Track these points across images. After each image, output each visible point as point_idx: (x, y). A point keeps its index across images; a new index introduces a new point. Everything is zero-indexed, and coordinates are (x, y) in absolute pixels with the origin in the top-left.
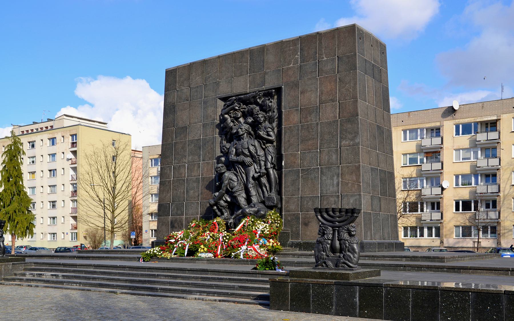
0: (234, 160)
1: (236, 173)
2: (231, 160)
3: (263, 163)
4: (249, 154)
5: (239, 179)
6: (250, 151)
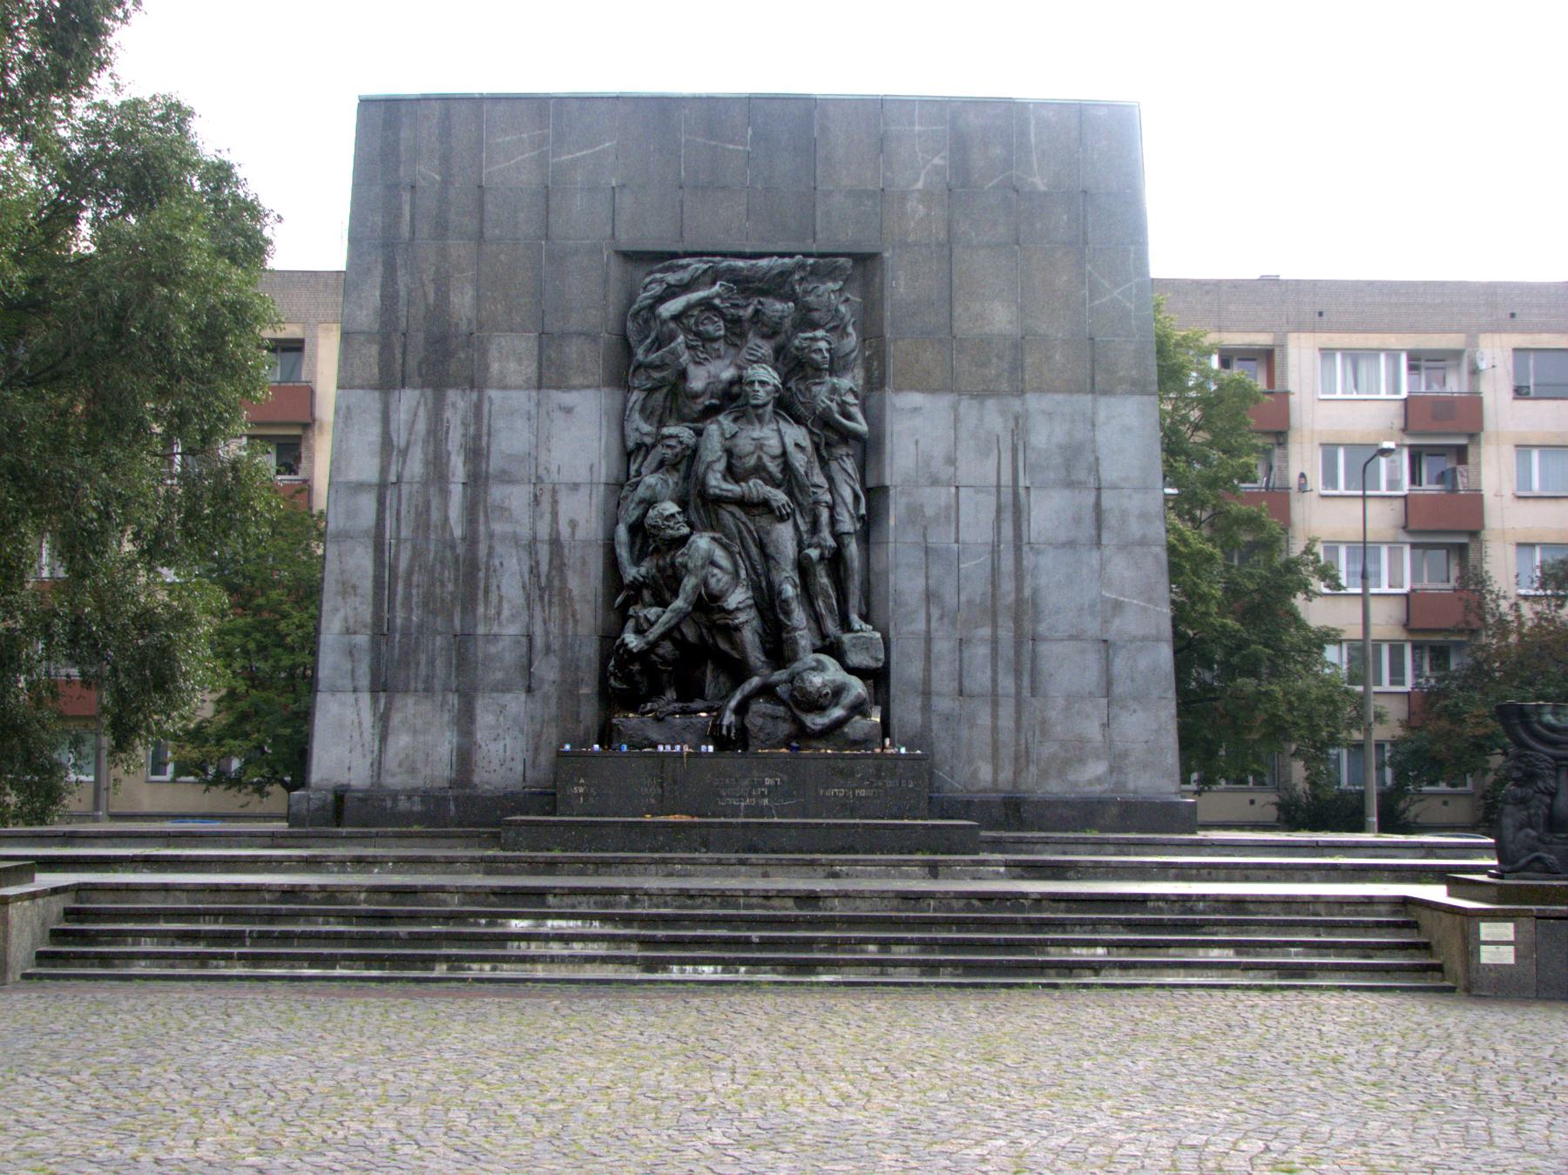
0: (730, 494)
1: (725, 540)
2: (717, 491)
3: (825, 515)
4: (780, 476)
5: (740, 562)
6: (787, 467)
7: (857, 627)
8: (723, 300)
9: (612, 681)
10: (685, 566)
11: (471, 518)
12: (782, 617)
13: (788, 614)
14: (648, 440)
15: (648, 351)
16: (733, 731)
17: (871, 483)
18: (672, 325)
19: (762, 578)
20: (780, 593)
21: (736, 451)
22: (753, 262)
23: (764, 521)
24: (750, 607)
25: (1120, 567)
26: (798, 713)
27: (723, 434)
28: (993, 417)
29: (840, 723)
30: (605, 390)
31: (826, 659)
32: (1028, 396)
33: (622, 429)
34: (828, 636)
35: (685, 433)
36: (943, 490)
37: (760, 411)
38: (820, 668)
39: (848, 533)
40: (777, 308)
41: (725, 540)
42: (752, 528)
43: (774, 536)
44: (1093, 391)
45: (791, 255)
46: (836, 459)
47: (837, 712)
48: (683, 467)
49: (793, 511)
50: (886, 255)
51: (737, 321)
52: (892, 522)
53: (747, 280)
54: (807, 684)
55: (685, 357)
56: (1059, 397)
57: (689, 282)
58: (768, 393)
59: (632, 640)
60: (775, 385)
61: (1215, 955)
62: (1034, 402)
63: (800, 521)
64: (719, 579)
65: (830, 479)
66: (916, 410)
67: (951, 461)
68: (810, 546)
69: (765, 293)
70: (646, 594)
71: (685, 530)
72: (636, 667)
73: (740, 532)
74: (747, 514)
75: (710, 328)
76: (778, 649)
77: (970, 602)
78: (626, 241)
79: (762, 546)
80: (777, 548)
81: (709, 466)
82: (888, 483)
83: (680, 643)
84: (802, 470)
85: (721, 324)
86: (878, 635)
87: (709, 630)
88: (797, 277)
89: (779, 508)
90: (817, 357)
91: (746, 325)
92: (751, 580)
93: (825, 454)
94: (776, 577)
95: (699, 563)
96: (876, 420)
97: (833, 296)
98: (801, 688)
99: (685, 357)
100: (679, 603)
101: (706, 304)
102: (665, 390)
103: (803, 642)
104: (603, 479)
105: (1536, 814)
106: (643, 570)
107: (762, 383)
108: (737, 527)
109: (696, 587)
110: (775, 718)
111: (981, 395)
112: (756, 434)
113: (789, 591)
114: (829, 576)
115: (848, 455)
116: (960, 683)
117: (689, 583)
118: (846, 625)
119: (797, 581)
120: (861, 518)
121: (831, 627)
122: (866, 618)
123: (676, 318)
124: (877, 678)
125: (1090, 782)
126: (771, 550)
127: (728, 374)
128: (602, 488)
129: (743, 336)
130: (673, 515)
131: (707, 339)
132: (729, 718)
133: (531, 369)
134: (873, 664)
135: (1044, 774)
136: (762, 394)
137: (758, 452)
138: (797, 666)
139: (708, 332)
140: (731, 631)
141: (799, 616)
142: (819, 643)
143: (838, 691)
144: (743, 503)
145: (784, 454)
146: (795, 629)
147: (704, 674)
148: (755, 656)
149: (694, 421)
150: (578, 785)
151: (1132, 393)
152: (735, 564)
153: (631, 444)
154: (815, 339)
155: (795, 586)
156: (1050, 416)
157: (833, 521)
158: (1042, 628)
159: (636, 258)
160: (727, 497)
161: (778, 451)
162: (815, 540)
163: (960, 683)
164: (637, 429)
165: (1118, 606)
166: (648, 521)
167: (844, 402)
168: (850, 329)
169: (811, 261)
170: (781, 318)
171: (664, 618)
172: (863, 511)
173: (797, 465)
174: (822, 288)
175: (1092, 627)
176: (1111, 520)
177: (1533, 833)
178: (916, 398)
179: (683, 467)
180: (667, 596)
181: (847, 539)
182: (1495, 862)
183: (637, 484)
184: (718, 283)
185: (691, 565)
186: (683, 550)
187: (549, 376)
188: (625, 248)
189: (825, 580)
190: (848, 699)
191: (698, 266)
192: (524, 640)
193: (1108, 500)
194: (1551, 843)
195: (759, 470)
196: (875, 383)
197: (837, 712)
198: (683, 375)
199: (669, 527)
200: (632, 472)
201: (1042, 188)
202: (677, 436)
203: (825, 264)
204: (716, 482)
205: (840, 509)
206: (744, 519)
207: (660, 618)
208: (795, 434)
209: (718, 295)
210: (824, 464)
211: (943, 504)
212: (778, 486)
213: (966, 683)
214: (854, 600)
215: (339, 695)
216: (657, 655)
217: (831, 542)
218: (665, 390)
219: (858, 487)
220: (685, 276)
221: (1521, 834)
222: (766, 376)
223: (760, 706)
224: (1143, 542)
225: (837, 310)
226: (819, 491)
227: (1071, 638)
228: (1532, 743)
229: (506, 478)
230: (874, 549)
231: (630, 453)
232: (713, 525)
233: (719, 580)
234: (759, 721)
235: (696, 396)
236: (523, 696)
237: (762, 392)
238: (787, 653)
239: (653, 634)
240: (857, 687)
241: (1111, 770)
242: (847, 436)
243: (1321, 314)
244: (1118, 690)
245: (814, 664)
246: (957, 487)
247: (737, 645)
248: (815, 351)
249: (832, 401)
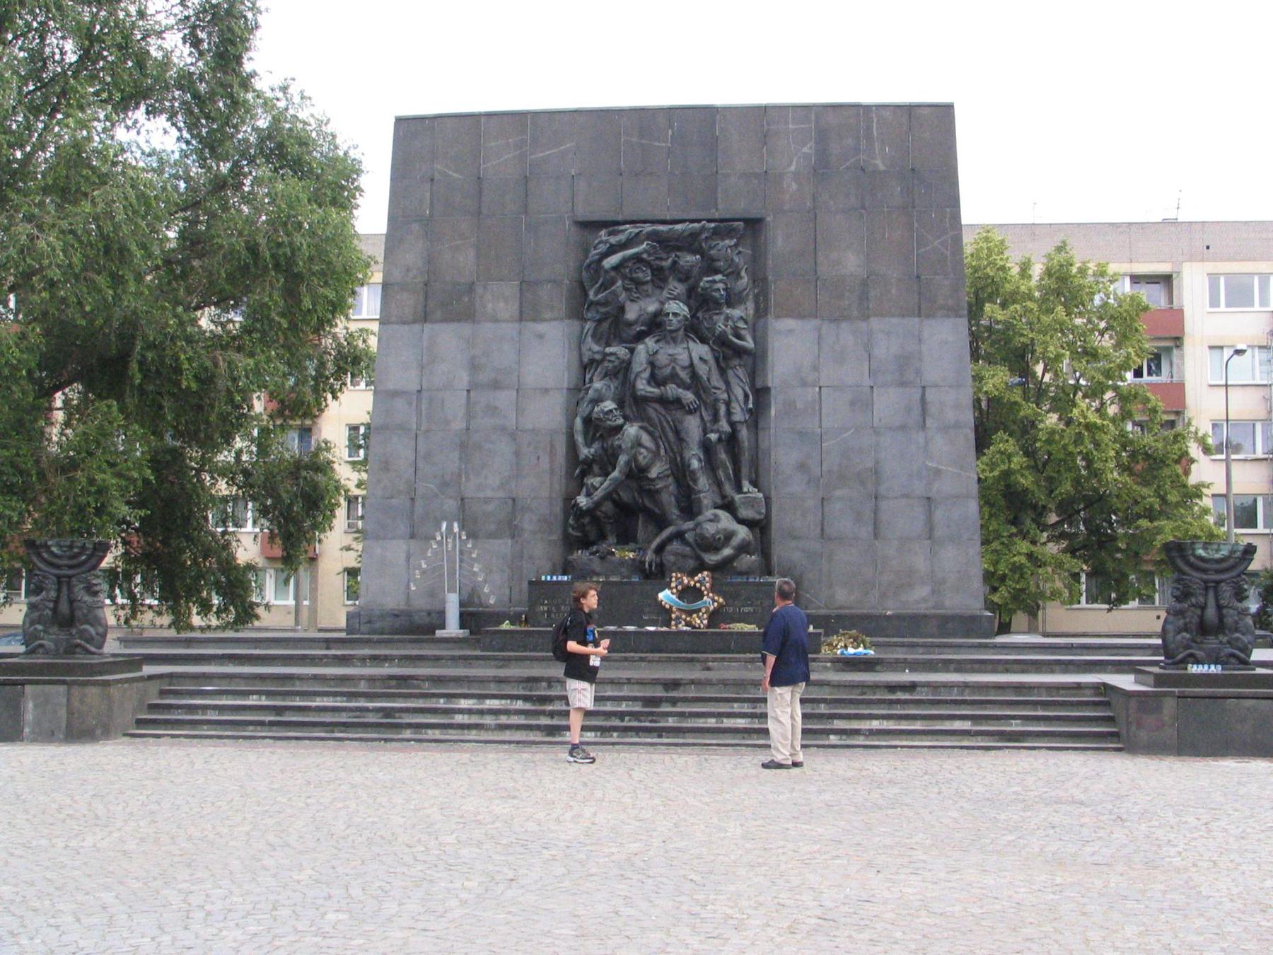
2: (643, 393)
6: (694, 375)
7: (745, 490)
8: (650, 255)
9: (570, 530)
10: (620, 447)
11: (469, 415)
12: (691, 483)
13: (695, 481)
14: (598, 357)
15: (596, 294)
16: (654, 565)
17: (759, 384)
18: (613, 274)
20: (689, 466)
21: (657, 363)
22: (671, 226)
23: (679, 414)
24: (668, 476)
25: (940, 444)
26: (699, 552)
27: (648, 352)
28: (846, 335)
29: (728, 561)
30: (567, 321)
31: (720, 512)
32: (872, 319)
33: (580, 349)
35: (620, 350)
36: (810, 390)
37: (674, 335)
38: (715, 519)
39: (740, 422)
40: (688, 259)
42: (669, 419)
43: (686, 424)
44: (919, 315)
45: (699, 221)
46: (732, 368)
47: (727, 552)
48: (621, 376)
50: (768, 219)
51: (661, 269)
52: (773, 412)
53: (668, 240)
54: (705, 532)
55: (623, 296)
56: (895, 320)
57: (626, 242)
58: (679, 322)
59: (582, 501)
60: (685, 316)
61: (958, 725)
62: (875, 323)
63: (704, 414)
64: (643, 457)
65: (727, 383)
66: (791, 331)
67: (816, 368)
68: (712, 431)
69: (679, 249)
70: (596, 468)
71: (620, 421)
72: (586, 520)
74: (665, 408)
75: (641, 275)
76: (690, 509)
77: (829, 471)
78: (583, 213)
79: (677, 432)
80: (686, 433)
81: (637, 375)
82: (770, 385)
83: (618, 504)
85: (649, 272)
86: (761, 495)
87: (639, 493)
88: (703, 236)
90: (716, 294)
91: (667, 273)
93: (723, 365)
94: (687, 455)
95: (630, 445)
96: (761, 340)
97: (729, 250)
99: (623, 296)
100: (615, 474)
101: (637, 258)
102: (609, 321)
103: (705, 502)
104: (566, 385)
105: (1190, 622)
106: (592, 450)
107: (675, 314)
108: (660, 421)
109: (628, 463)
110: (684, 556)
111: (835, 320)
112: (671, 351)
113: (695, 464)
114: (726, 452)
115: (740, 365)
116: (822, 530)
117: (622, 459)
118: (739, 489)
119: (702, 457)
120: (750, 411)
121: (728, 489)
122: (755, 483)
123: (616, 268)
124: (760, 527)
125: (917, 602)
126: (683, 435)
127: (652, 307)
128: (565, 391)
129: (665, 280)
130: (611, 411)
131: (638, 283)
132: (649, 556)
133: (514, 307)
134: (757, 517)
135: (884, 595)
136: (674, 323)
137: (673, 364)
138: (700, 518)
139: (638, 278)
140: (653, 494)
141: (703, 482)
142: (719, 501)
143: (729, 536)
144: (663, 401)
145: (692, 365)
146: (700, 492)
147: (637, 525)
148: (674, 512)
149: (631, 342)
150: (543, 605)
151: (948, 316)
152: (658, 447)
153: (586, 360)
154: (714, 282)
155: (700, 460)
156: (888, 334)
157: (729, 413)
158: (883, 489)
159: (590, 226)
161: (687, 363)
163: (822, 530)
164: (590, 350)
165: (938, 472)
166: (594, 416)
168: (743, 273)
169: (713, 225)
170: (692, 266)
171: (606, 484)
172: (751, 406)
173: (701, 373)
174: (721, 244)
175: (919, 488)
176: (933, 409)
177: (1188, 636)
178: (789, 323)
179: (621, 376)
180: (610, 469)
181: (739, 427)
182: (1163, 658)
183: (589, 388)
185: (623, 446)
186: (620, 436)
187: (527, 313)
188: (580, 219)
189: (723, 456)
190: (735, 541)
191: (630, 230)
192: (510, 502)
193: (931, 395)
194: (1202, 643)
195: (674, 377)
196: (762, 311)
197: (727, 552)
198: (622, 309)
200: (587, 380)
201: (882, 167)
203: (724, 228)
204: (643, 387)
205: (734, 405)
206: (663, 412)
207: (600, 484)
208: (700, 350)
209: (645, 251)
210: (722, 372)
211: (809, 399)
212: (687, 388)
213: (827, 530)
214: (745, 471)
215: (381, 542)
217: (727, 428)
218: (609, 321)
219: (747, 389)
220: (622, 237)
221: (1179, 637)
222: (678, 309)
223: (676, 546)
224: (957, 425)
225: (732, 260)
227: (905, 496)
228: (1186, 569)
229: (496, 385)
230: (761, 434)
231: (587, 366)
232: (641, 417)
233: (644, 457)
234: (672, 558)
235: (630, 324)
236: (510, 542)
237: (675, 320)
238: (695, 510)
239: (598, 495)
240: (743, 532)
241: (933, 592)
242: (740, 352)
243: (1208, 247)
244: (938, 533)
245: (712, 517)
246: (820, 388)
247: (658, 503)
249: (726, 326)
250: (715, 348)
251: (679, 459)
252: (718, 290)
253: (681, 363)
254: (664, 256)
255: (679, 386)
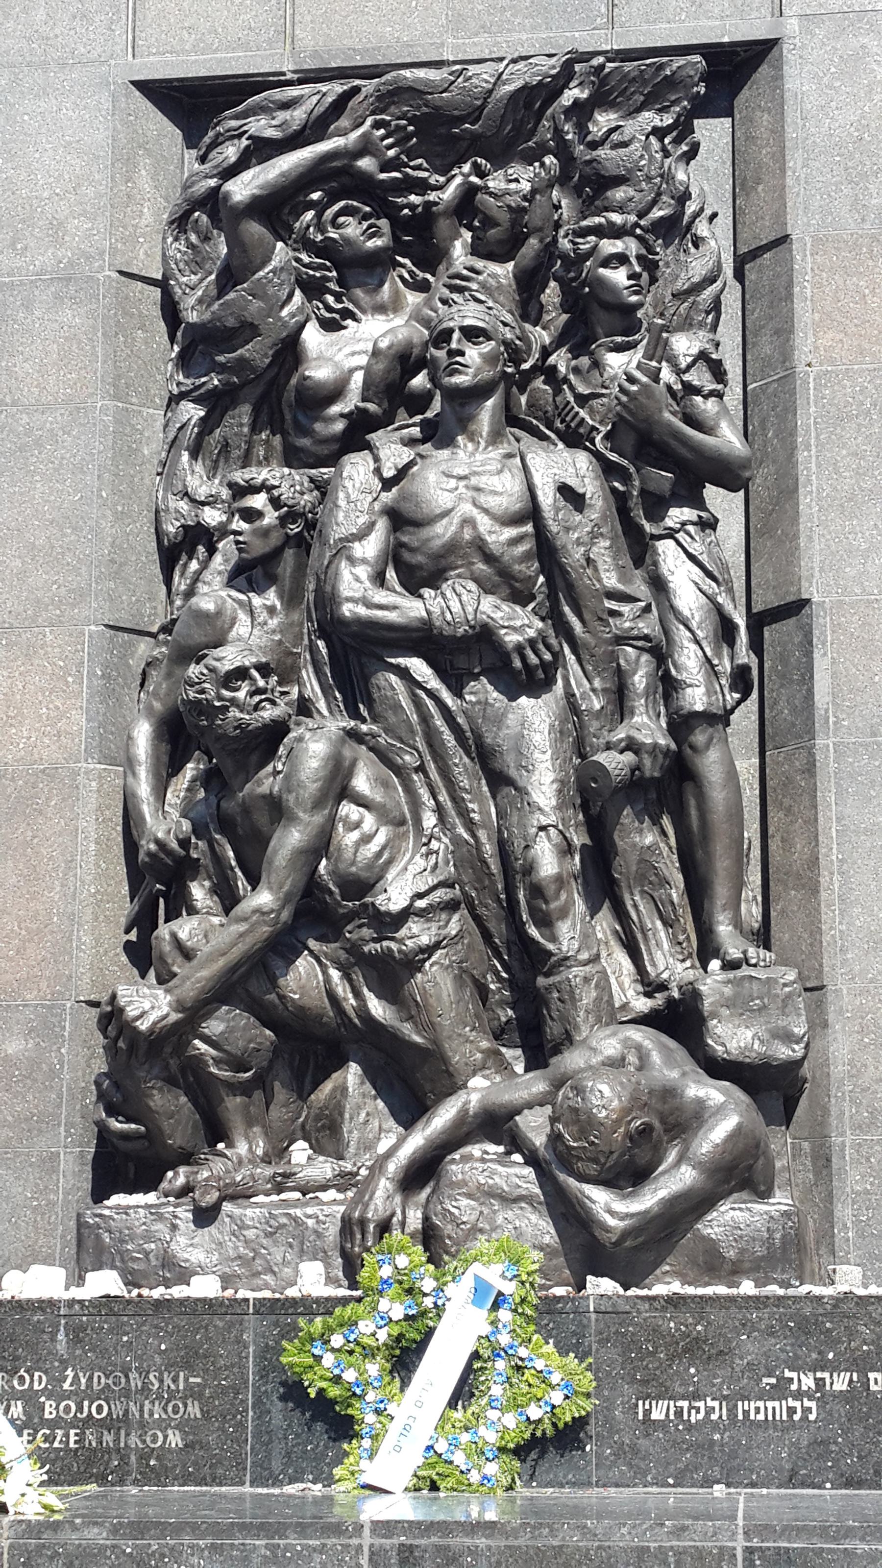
0: (391, 616)
5: (424, 794)
12: (533, 932)
19: (482, 835)
20: (529, 869)
21: (407, 509)
27: (378, 471)
34: (663, 987)
41: (384, 740)
49: (557, 656)
60: (506, 343)
68: (608, 747)
73: (425, 718)
81: (342, 549)
84: (578, 554)
85: (384, 223)
89: (519, 649)
90: (619, 277)
91: (443, 226)
92: (456, 841)
95: (312, 788)
98: (575, 1111)
107: (472, 334)
130: (241, 673)
139: (347, 240)
153: (171, 528)
155: (566, 849)
160: (390, 627)
162: (621, 734)
167: (691, 389)
184: (369, 121)
185: (290, 799)
199: (233, 701)
202: (265, 487)
206: (434, 683)
209: (365, 148)
216: (206, 1040)
225: (667, 177)
226: (625, 608)
248: (606, 262)
250: (613, 457)
251: (489, 849)
252: (621, 259)
253: (492, 502)
254: (436, 179)
255: (486, 588)
